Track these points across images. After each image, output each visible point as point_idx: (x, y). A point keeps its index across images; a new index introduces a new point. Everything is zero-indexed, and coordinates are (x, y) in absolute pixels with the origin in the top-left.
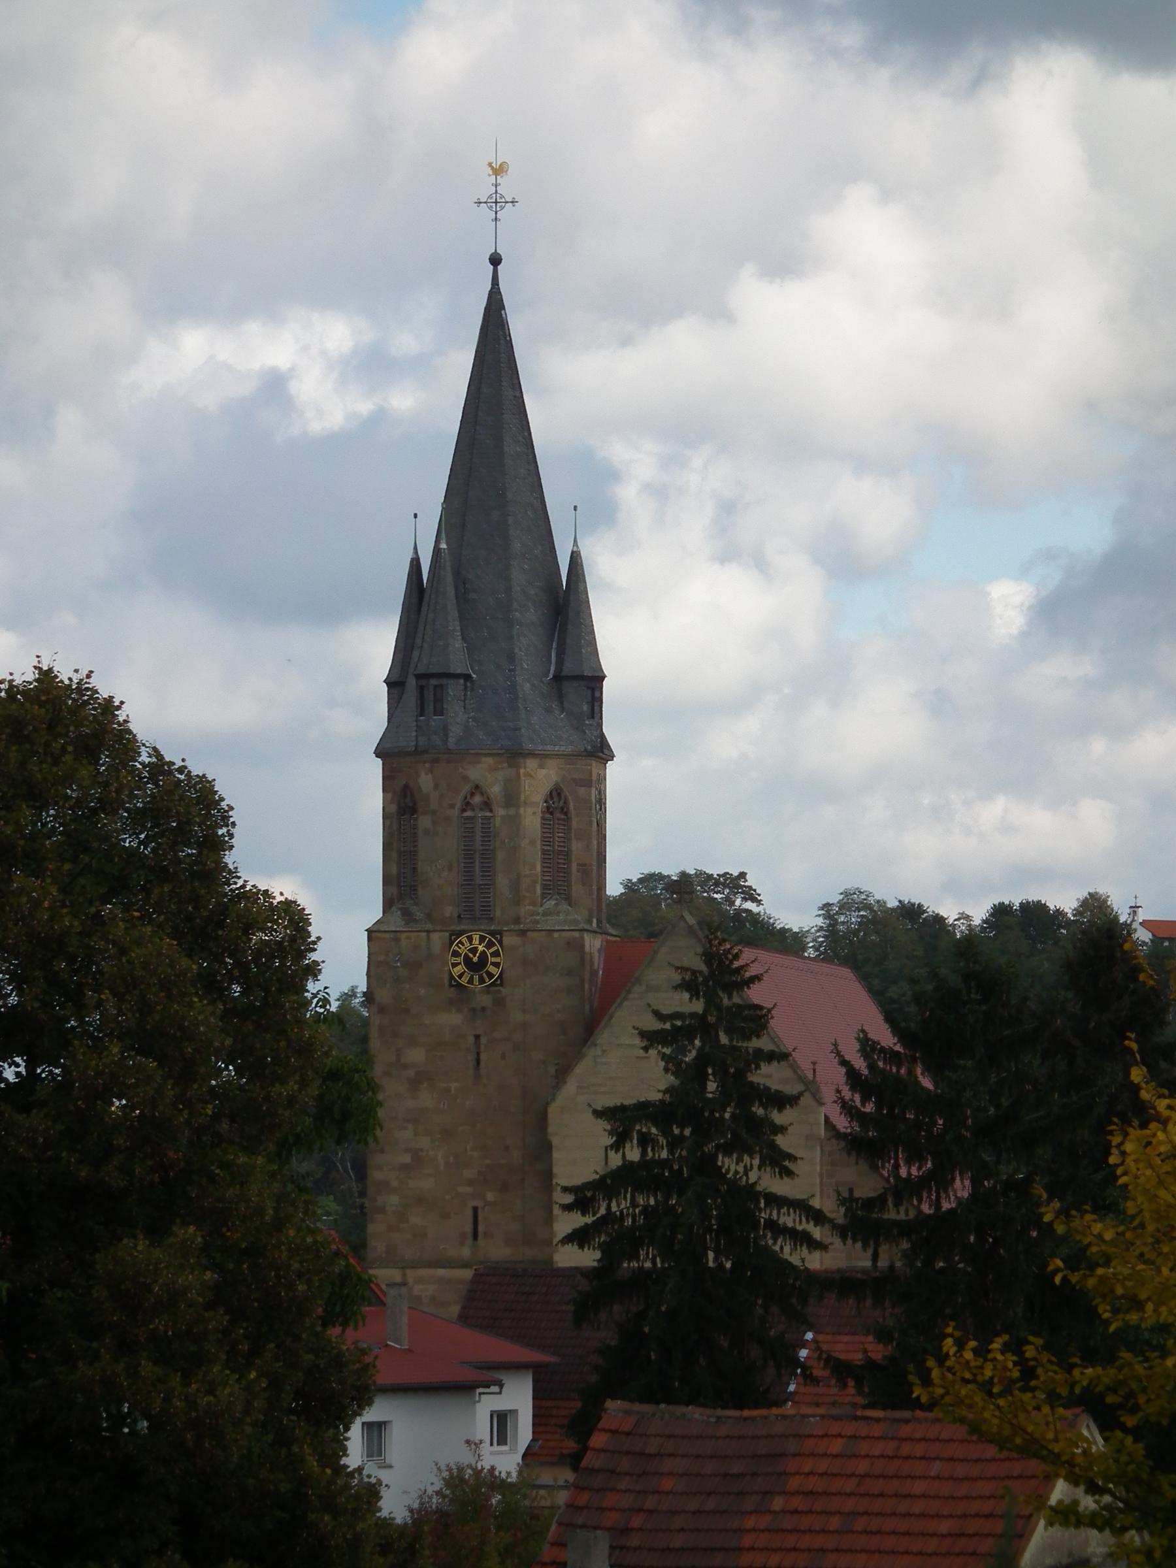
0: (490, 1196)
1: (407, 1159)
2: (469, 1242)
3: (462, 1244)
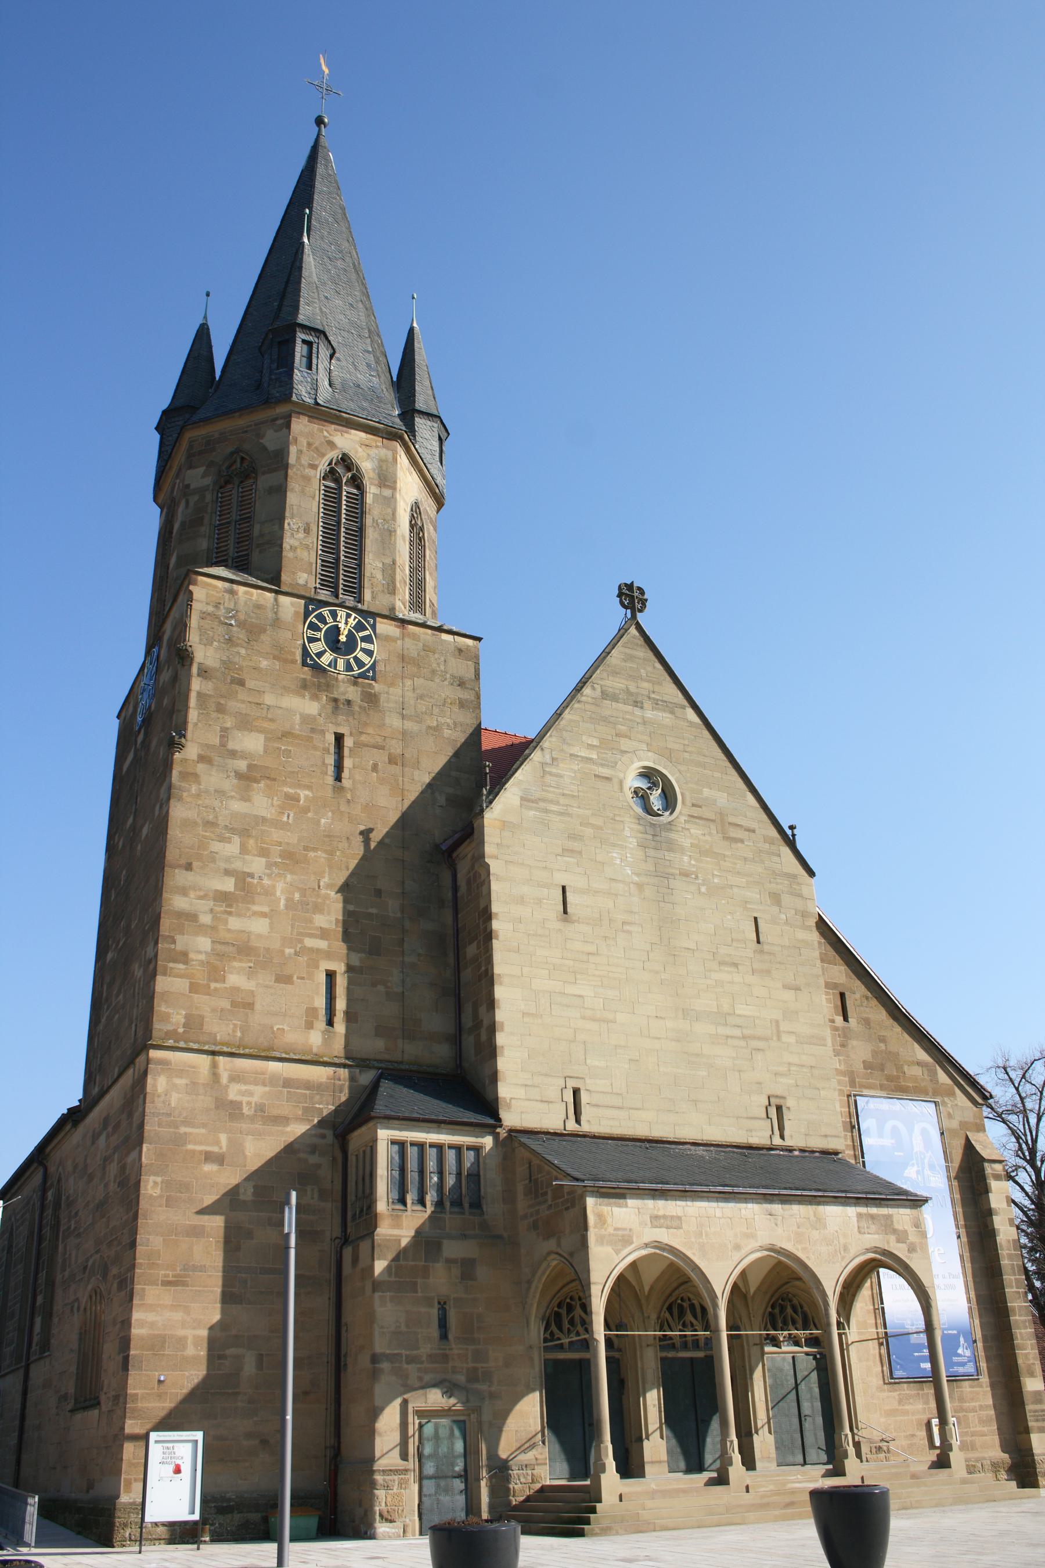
1: (228, 885)
2: (321, 1024)
3: (310, 1026)
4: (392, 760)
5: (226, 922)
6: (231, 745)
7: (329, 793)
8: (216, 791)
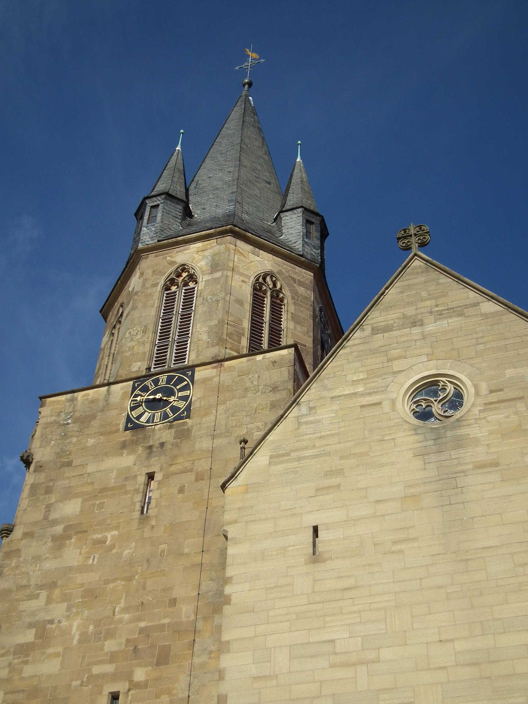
0: (140, 675)
4: (199, 477)
5: (21, 671)
6: (53, 516)
7: (135, 524)
8: (33, 558)
